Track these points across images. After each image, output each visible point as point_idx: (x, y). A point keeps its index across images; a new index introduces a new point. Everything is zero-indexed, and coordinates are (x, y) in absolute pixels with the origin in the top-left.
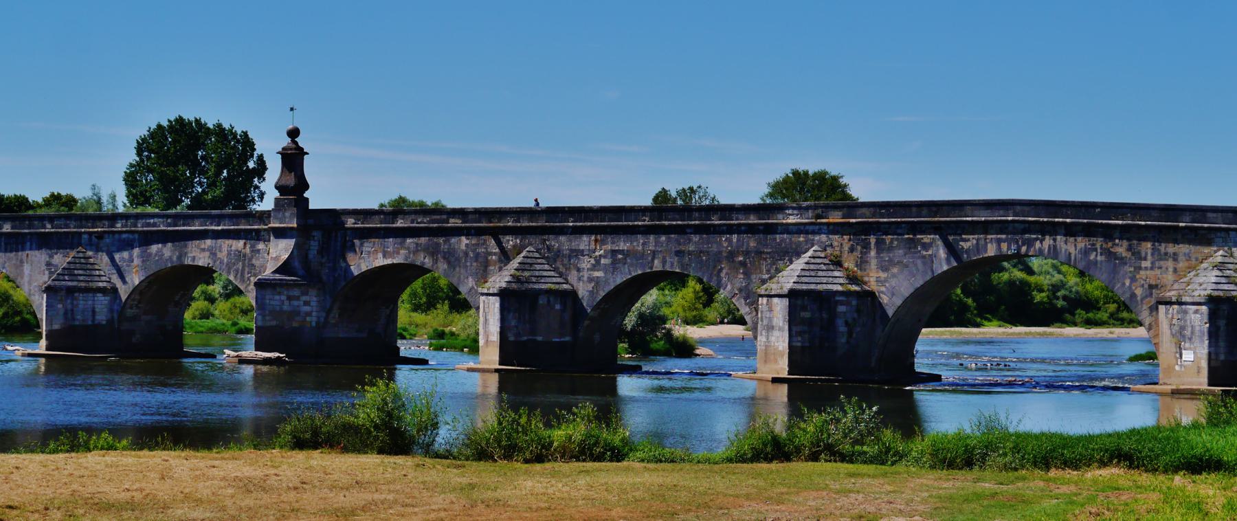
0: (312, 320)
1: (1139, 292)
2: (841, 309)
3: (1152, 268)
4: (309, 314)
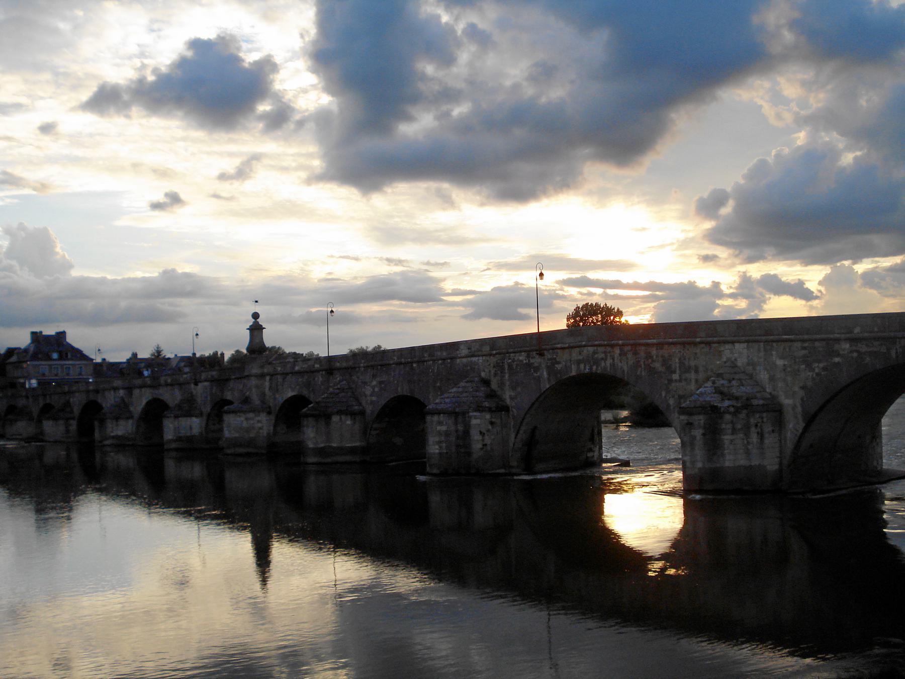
0: (264, 432)
1: (671, 402)
2: (474, 422)
3: (680, 381)
4: (260, 428)
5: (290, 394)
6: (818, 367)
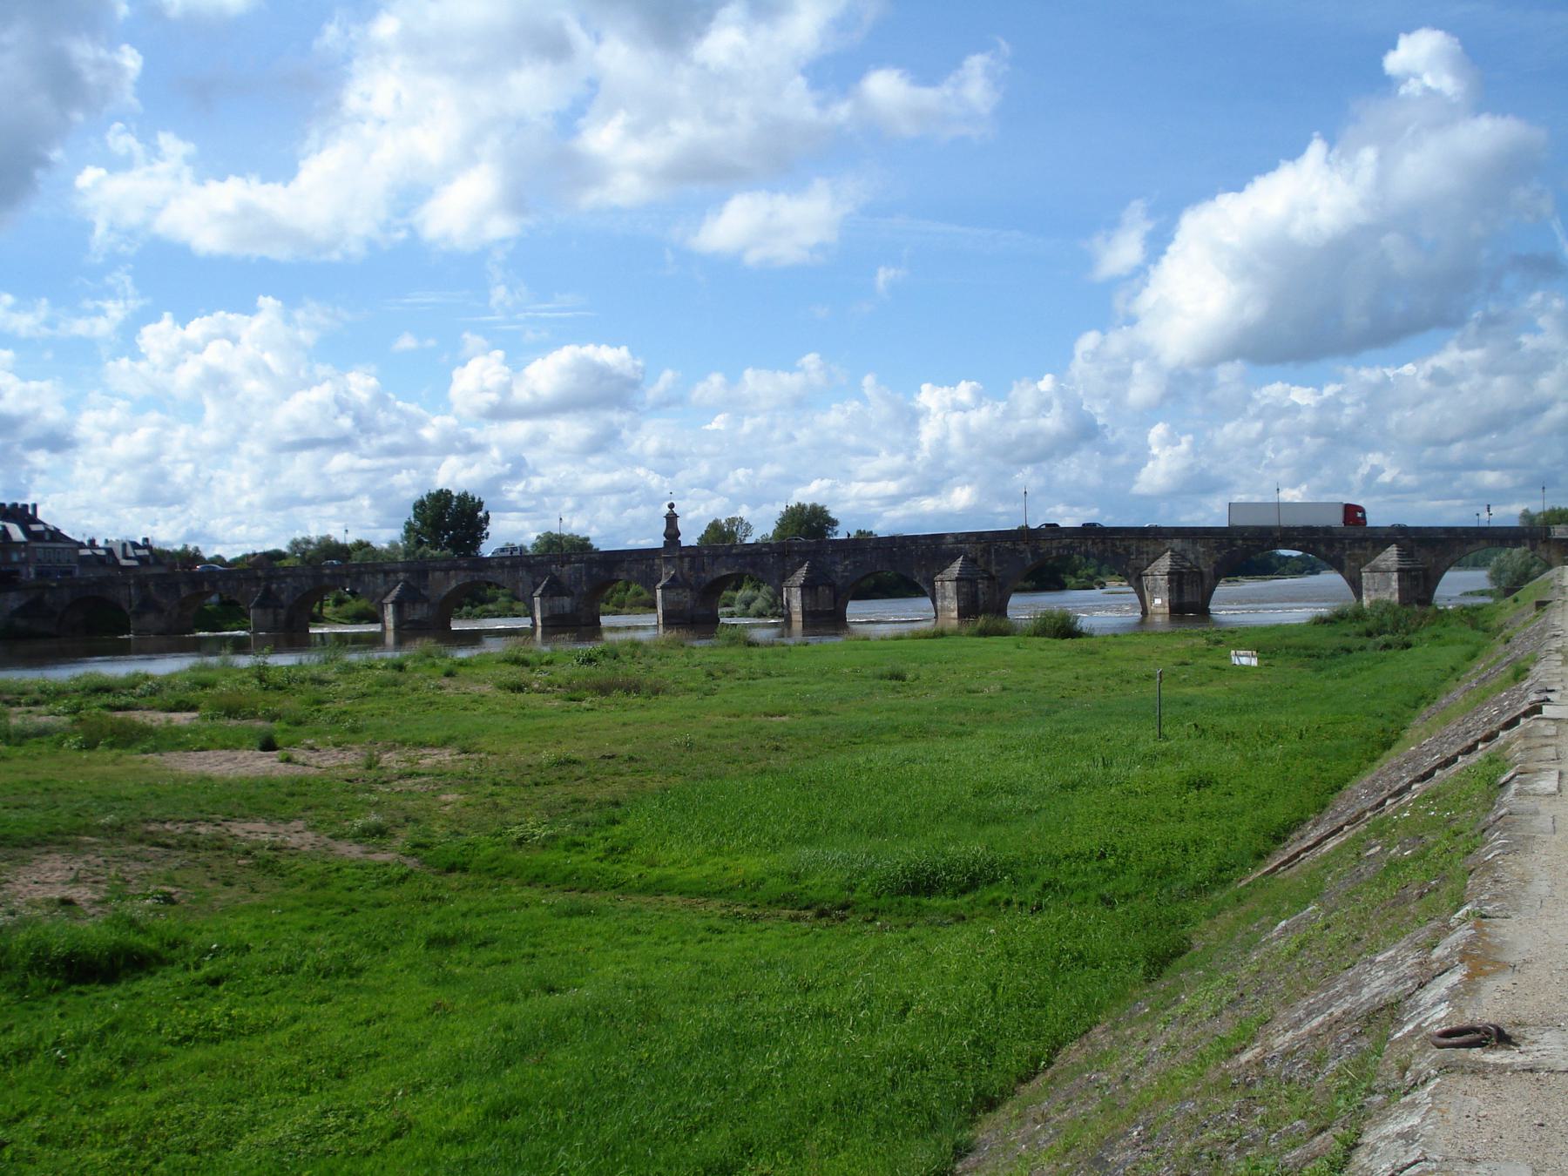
5: (724, 572)
6: (1224, 552)
